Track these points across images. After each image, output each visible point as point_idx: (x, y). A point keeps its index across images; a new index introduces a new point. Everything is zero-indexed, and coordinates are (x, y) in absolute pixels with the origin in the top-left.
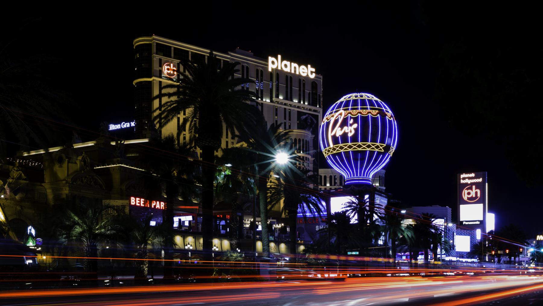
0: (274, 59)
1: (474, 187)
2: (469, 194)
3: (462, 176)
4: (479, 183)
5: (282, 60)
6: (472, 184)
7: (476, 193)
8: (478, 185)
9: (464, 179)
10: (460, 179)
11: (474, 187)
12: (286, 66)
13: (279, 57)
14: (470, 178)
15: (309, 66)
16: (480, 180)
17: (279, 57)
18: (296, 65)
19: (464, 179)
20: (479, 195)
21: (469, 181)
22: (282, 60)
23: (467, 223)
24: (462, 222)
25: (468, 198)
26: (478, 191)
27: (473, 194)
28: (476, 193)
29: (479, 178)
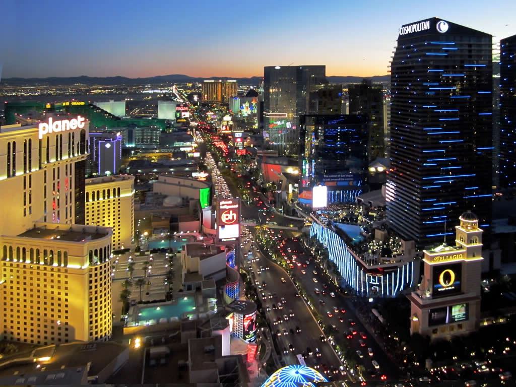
0: (45, 124)
1: (231, 212)
2: (227, 217)
3: (222, 203)
4: (235, 208)
5: (53, 121)
6: (230, 209)
7: (233, 216)
8: (234, 210)
9: (223, 205)
10: (220, 205)
11: (231, 212)
12: (57, 126)
13: (51, 119)
14: (228, 205)
15: (79, 117)
16: (236, 206)
17: (51, 119)
18: (66, 121)
19: (223, 205)
20: (235, 218)
21: (227, 207)
22: (53, 121)
23: (225, 240)
24: (221, 239)
25: (227, 221)
26: (235, 215)
27: (230, 217)
28: (233, 216)
29: (236, 205)
